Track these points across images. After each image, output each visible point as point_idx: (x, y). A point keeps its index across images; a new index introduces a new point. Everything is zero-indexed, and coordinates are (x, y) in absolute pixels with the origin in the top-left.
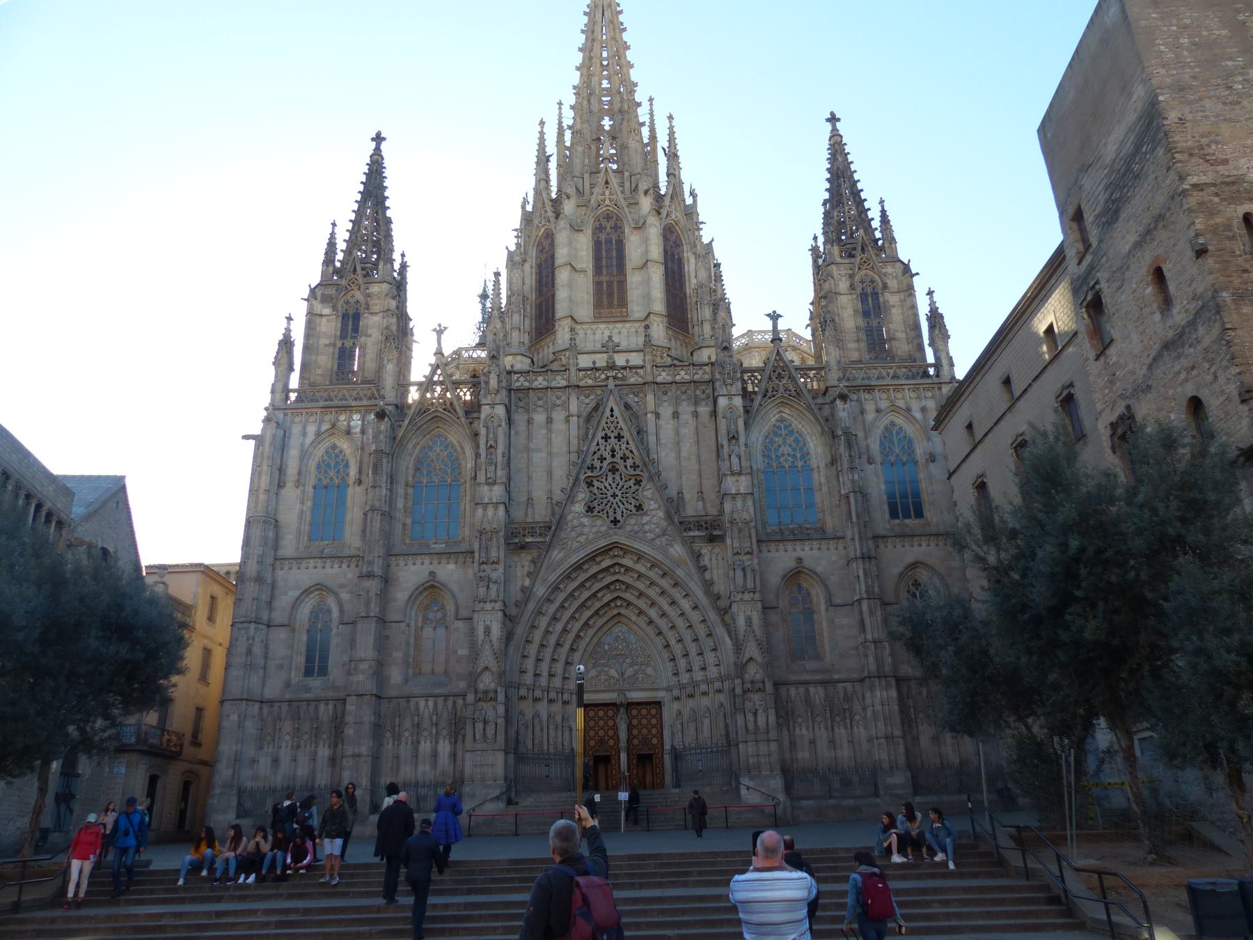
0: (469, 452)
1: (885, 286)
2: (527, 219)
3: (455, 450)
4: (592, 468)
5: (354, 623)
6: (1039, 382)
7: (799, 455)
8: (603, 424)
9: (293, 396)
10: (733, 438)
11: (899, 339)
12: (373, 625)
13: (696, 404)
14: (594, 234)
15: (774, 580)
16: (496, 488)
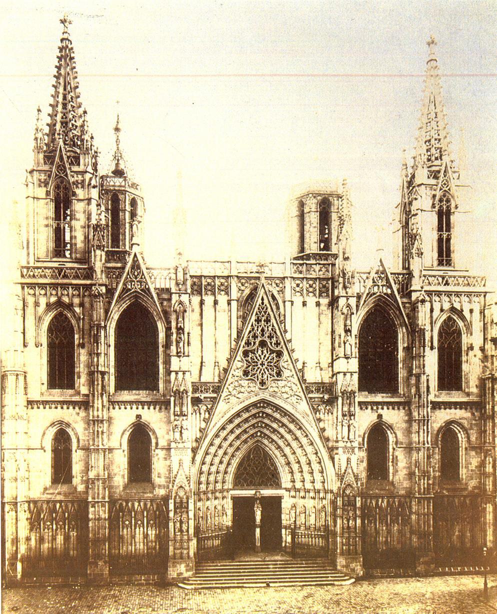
8: (256, 309)
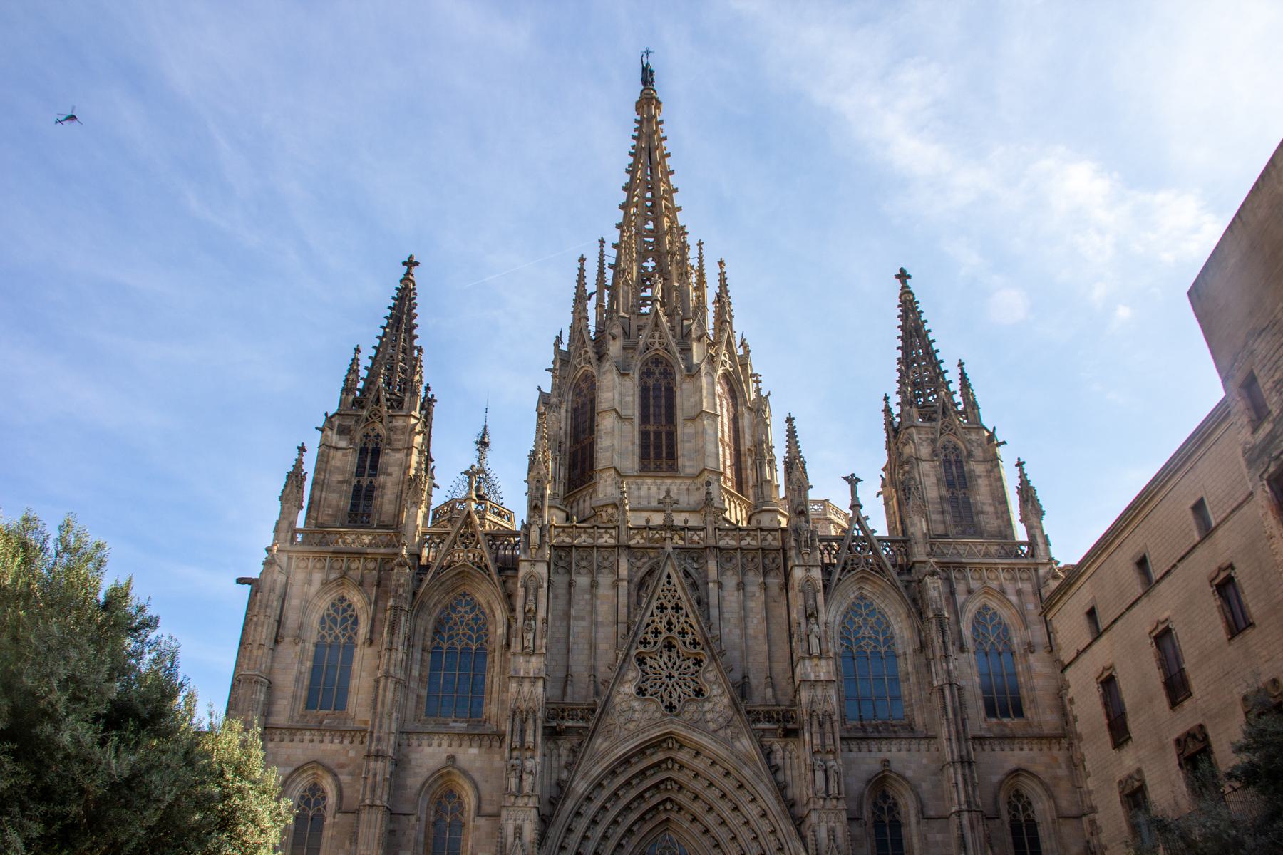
0: (500, 614)
1: (970, 455)
2: (563, 360)
3: (483, 613)
4: (645, 643)
5: (357, 812)
6: (1185, 562)
7: (881, 639)
8: (659, 591)
9: (299, 537)
10: (811, 616)
11: (987, 513)
12: (380, 816)
13: (765, 575)
14: (641, 379)
15: (857, 785)
16: (534, 659)
